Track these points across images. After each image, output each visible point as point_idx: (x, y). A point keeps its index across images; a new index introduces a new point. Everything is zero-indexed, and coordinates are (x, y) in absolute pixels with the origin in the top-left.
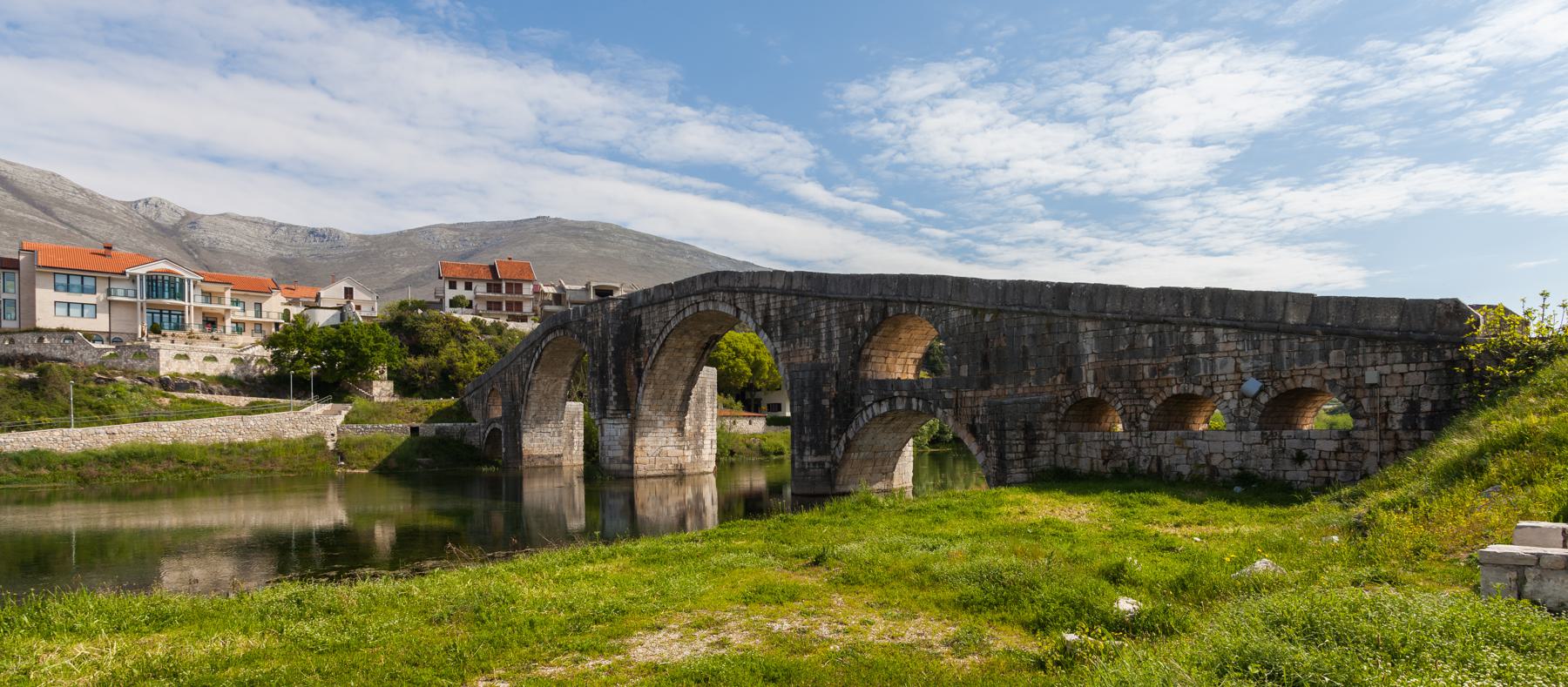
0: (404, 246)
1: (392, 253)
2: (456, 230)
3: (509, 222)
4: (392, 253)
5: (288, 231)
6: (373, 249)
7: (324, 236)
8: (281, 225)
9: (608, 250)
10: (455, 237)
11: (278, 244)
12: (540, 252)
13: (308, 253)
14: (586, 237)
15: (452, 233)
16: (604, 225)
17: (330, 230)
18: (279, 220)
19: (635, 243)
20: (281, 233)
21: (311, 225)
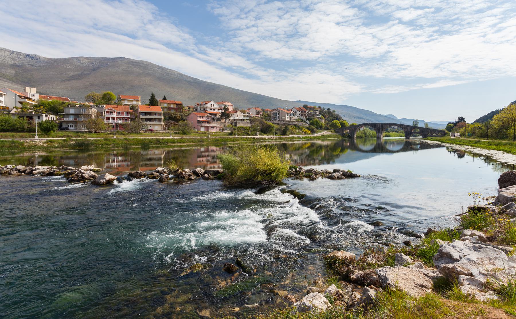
0: (68, 64)
1: (64, 66)
2: (89, 59)
3: (109, 58)
4: (64, 66)
5: (17, 54)
6: (55, 64)
7: (33, 57)
8: (13, 52)
9: (149, 71)
10: (89, 62)
11: (13, 59)
12: (125, 70)
13: (27, 64)
14: (140, 66)
15: (87, 60)
16: (146, 62)
17: (36, 56)
18: (13, 49)
19: (158, 69)
20: (14, 55)
21: (27, 53)
